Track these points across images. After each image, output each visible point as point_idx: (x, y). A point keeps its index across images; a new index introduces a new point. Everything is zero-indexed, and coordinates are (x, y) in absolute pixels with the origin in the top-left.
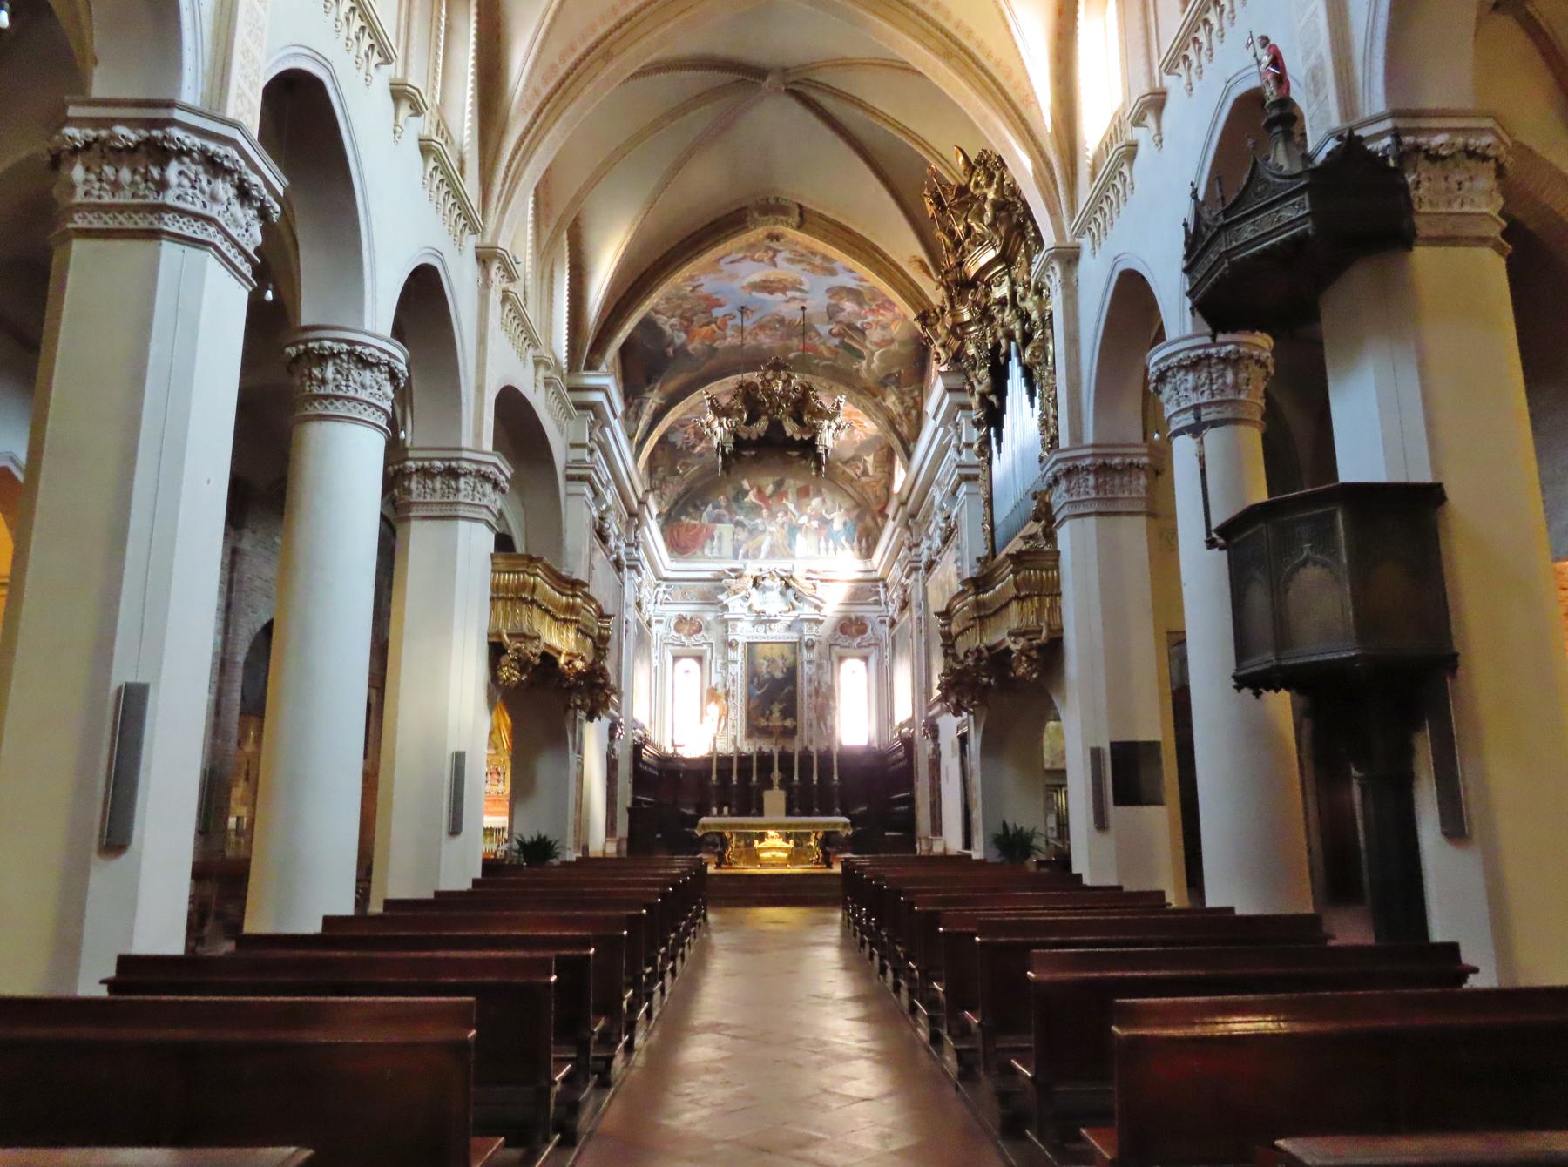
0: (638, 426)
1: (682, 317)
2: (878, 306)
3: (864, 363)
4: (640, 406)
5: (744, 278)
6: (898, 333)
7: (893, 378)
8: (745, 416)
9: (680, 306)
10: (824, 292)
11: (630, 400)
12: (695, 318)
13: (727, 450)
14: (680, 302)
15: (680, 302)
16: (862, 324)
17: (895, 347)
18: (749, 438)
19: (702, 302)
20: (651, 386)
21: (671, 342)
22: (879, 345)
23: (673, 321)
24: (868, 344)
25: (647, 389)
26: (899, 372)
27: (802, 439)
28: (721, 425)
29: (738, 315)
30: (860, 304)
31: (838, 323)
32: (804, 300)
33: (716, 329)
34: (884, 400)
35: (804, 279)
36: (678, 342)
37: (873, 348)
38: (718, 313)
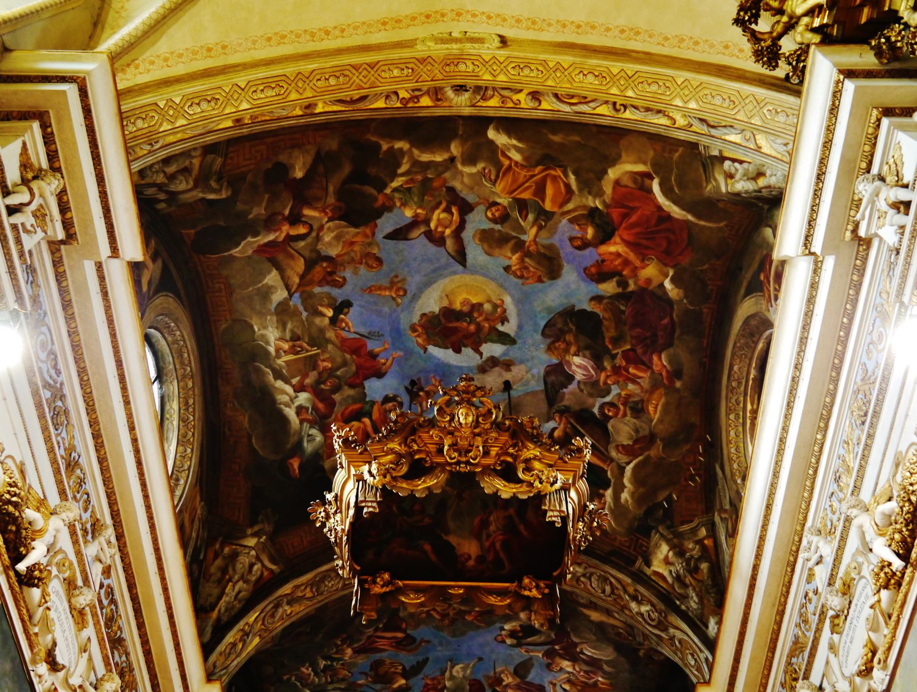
0: (222, 593)
1: (316, 391)
2: (625, 354)
3: (609, 493)
4: (234, 556)
5: (416, 297)
6: (661, 421)
7: (661, 512)
8: (405, 469)
9: (312, 362)
10: (538, 337)
11: (217, 546)
12: (337, 397)
13: (365, 510)
14: (315, 351)
15: (315, 351)
16: (602, 407)
17: (656, 451)
18: (412, 496)
19: (348, 356)
20: (256, 528)
21: (298, 447)
22: (630, 451)
23: (304, 398)
24: (614, 454)
25: (249, 531)
26: (669, 499)
27: (514, 497)
28: (360, 478)
29: (405, 398)
30: (597, 360)
31: (564, 412)
32: (508, 365)
33: (370, 429)
34: (648, 564)
35: (508, 300)
36: (308, 447)
37: (623, 459)
38: (376, 389)
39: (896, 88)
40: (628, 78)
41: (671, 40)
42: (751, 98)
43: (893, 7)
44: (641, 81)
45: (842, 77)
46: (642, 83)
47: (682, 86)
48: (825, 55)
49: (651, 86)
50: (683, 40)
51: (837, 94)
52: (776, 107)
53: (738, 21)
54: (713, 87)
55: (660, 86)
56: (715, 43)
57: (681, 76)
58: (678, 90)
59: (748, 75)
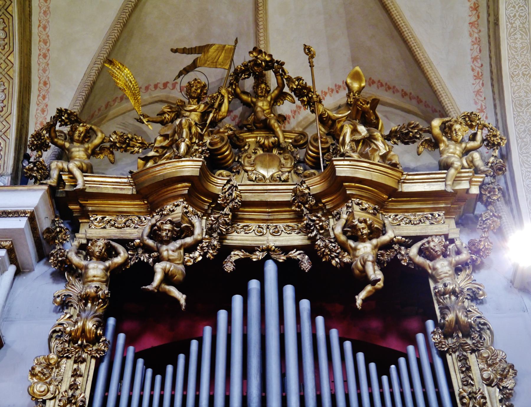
39: (28, 250)
40: (5, 7)
41: (44, 33)
42: (7, 126)
43: (81, 225)
44: (5, 21)
45: (28, 215)
46: (4, 22)
47: (7, 61)
48: (42, 197)
49: (2, 32)
50: (46, 43)
51: (16, 214)
52: (3, 149)
53: (60, 112)
54: (11, 90)
55: (4, 39)
56: (47, 72)
57: (15, 60)
58: (4, 58)
59: (26, 112)
